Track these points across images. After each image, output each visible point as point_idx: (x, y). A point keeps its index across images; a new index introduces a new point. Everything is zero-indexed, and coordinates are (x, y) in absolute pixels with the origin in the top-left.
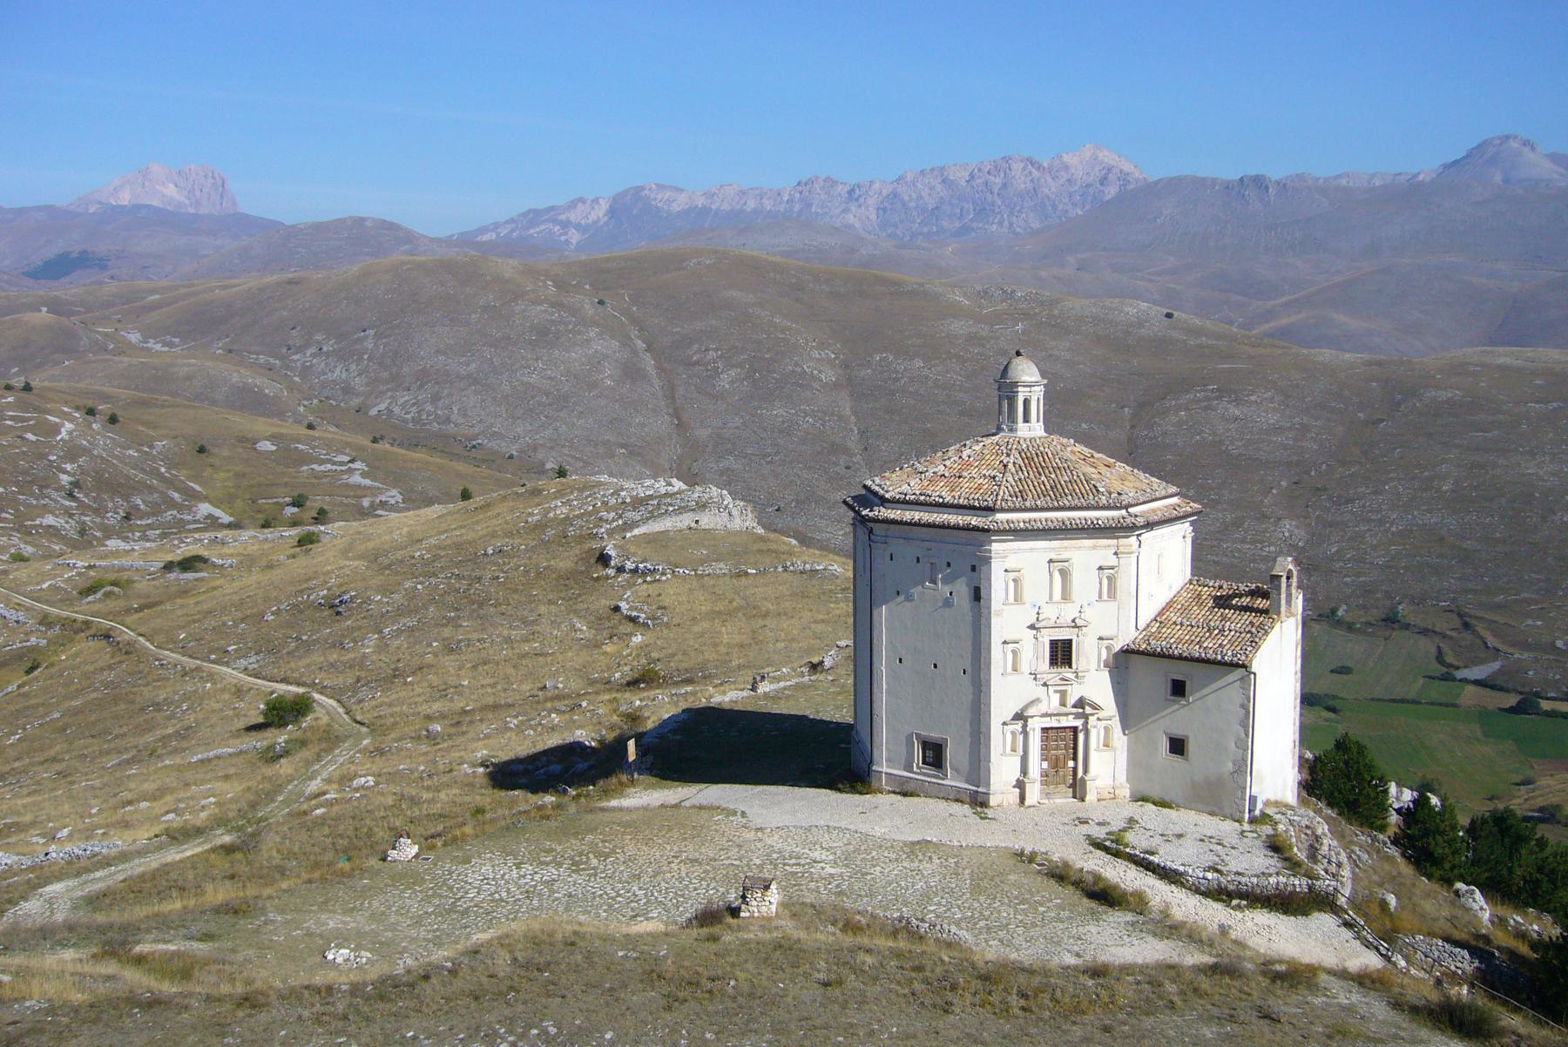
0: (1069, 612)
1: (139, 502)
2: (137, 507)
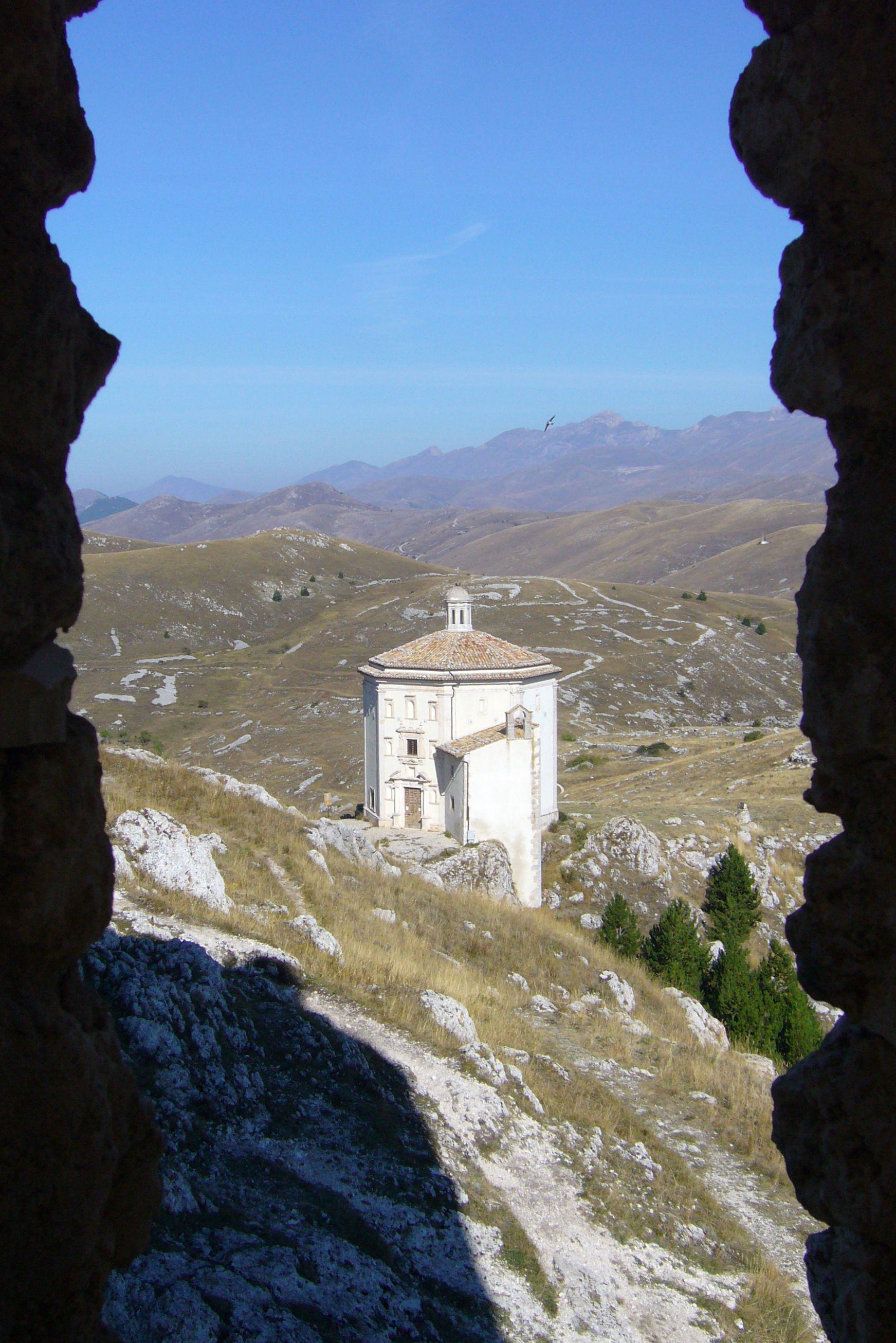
0: (415, 726)
1: (744, 706)
2: (739, 711)
